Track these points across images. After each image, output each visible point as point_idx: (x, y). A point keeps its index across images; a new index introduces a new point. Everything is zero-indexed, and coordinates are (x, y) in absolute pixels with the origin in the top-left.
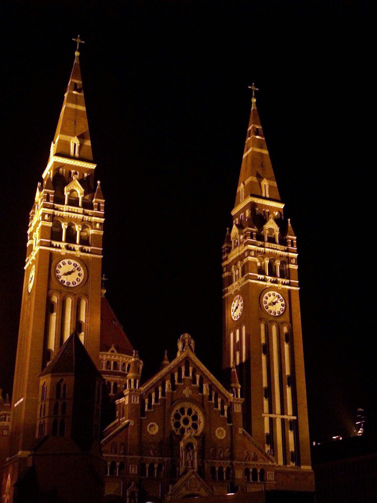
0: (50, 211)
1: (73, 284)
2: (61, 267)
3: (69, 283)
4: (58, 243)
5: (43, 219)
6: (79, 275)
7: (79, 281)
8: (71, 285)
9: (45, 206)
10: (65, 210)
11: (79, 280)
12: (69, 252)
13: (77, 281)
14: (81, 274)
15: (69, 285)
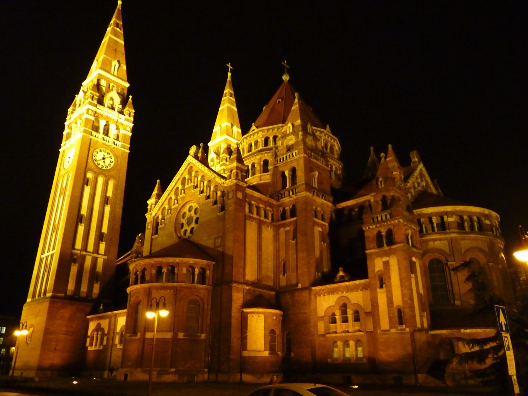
0: (94, 108)
1: (106, 167)
2: (98, 153)
3: (103, 166)
4: (97, 134)
5: (88, 113)
6: (111, 162)
7: (110, 166)
8: (104, 168)
9: (90, 103)
10: (103, 110)
11: (110, 165)
12: (104, 142)
13: (109, 166)
14: (112, 162)
15: (102, 167)
